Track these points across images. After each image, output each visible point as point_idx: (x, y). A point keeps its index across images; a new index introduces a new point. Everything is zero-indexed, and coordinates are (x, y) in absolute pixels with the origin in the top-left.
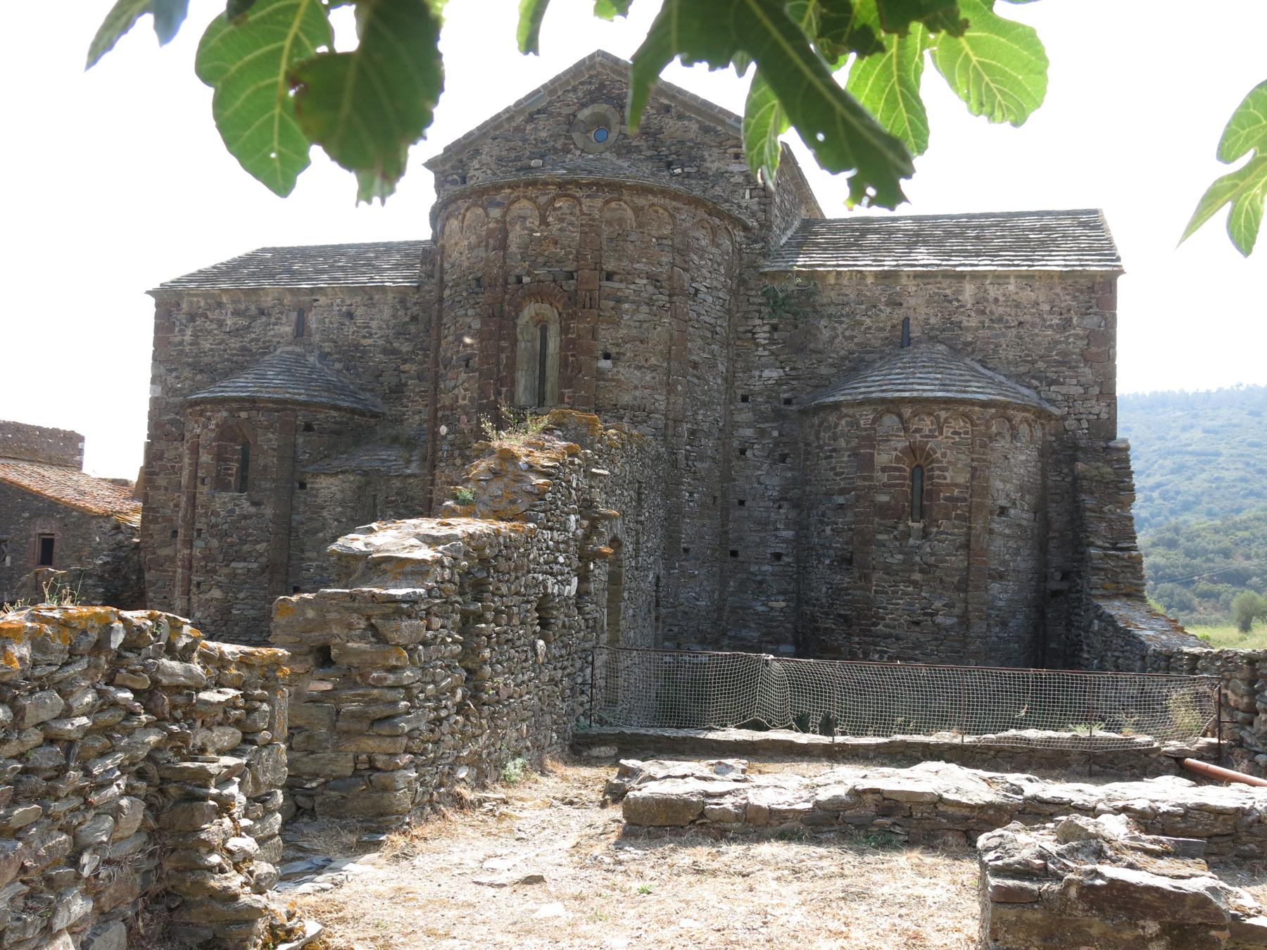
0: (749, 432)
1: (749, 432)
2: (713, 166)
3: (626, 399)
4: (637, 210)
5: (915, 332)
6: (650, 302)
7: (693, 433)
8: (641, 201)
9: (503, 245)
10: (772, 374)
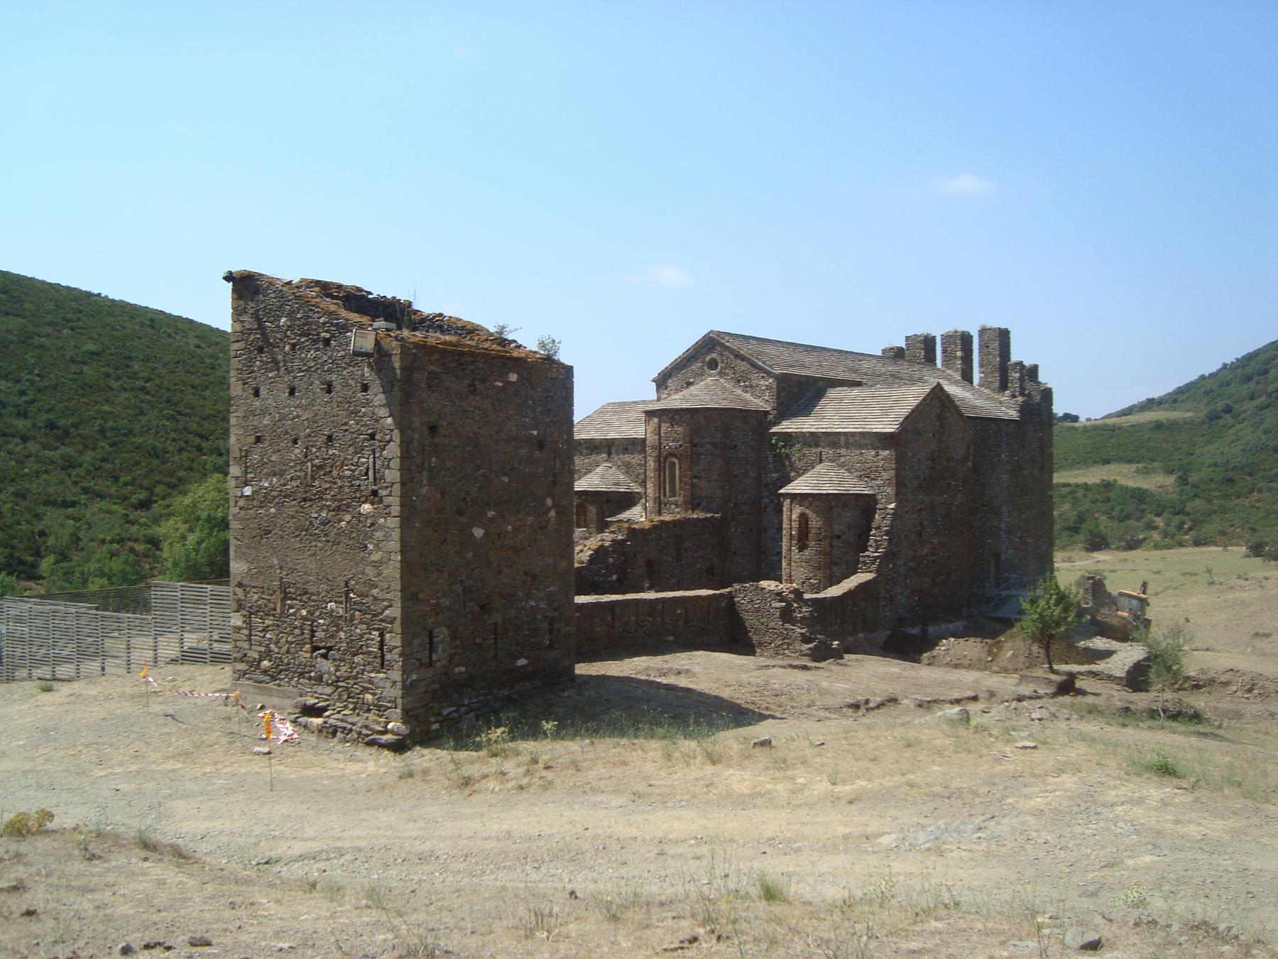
0: (766, 500)
1: (766, 500)
2: (754, 382)
3: (704, 494)
4: (705, 418)
5: (824, 457)
6: (712, 454)
7: (736, 505)
8: (706, 414)
9: (659, 434)
10: (775, 475)
